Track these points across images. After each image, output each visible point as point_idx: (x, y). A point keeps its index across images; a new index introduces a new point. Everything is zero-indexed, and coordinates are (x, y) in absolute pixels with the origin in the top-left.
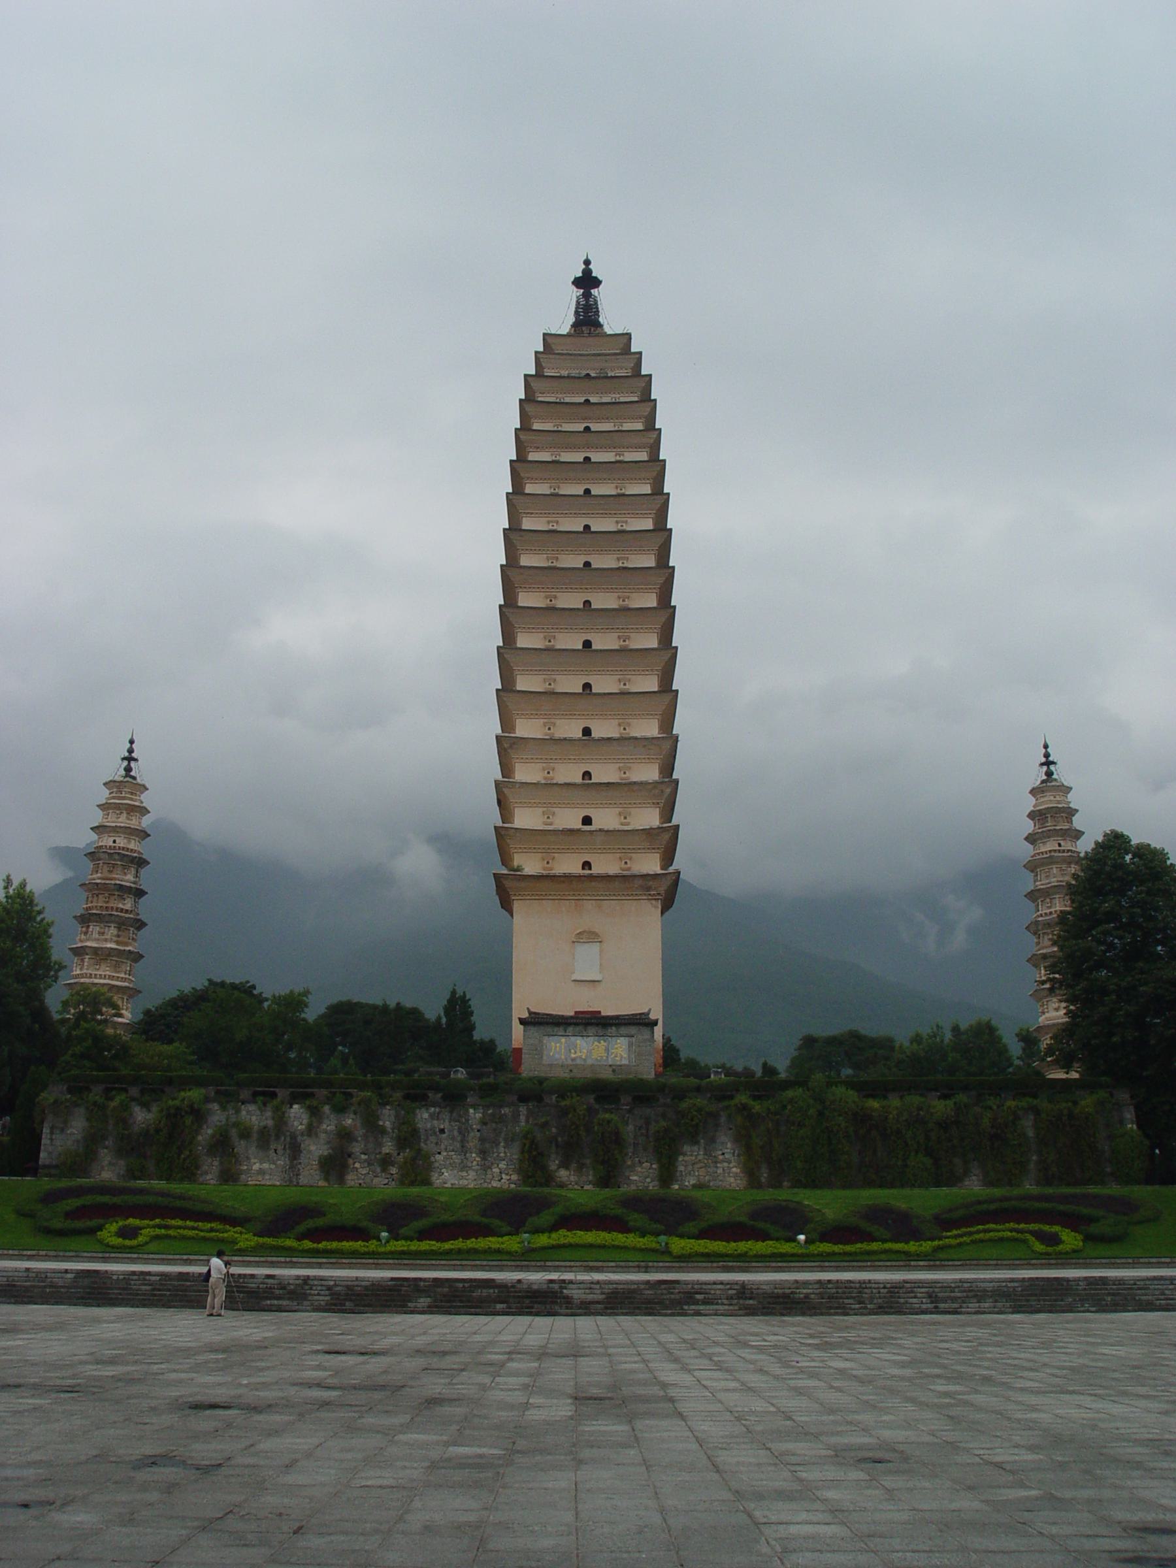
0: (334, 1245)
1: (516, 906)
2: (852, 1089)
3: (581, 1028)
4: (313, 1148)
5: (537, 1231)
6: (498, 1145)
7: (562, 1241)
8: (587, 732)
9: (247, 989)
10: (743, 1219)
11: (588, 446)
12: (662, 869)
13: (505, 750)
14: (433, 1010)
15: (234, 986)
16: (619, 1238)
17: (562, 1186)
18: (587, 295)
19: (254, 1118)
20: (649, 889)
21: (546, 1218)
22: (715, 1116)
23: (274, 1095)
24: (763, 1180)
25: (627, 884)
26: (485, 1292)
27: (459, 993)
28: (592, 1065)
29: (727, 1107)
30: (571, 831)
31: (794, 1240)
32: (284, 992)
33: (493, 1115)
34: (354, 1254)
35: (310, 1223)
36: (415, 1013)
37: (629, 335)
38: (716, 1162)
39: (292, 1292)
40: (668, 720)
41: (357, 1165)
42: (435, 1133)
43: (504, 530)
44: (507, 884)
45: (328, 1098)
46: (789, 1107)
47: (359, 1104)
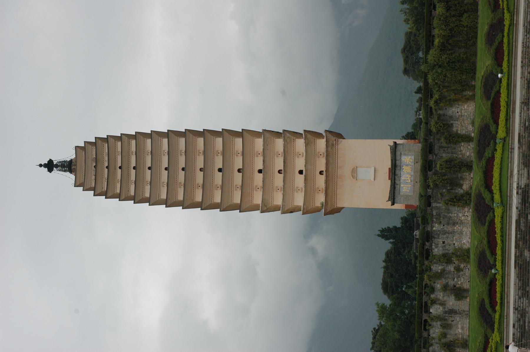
0: (498, 295)
1: (339, 205)
2: (429, 52)
3: (396, 177)
4: (451, 304)
5: (492, 199)
6: (451, 217)
7: (498, 188)
8: (260, 171)
9: (376, 331)
10: (489, 103)
11: (128, 167)
12: (323, 138)
13: (267, 209)
14: (387, 245)
15: (374, 338)
16: (497, 161)
17: (471, 188)
18: (57, 166)
19: (437, 331)
20: (333, 145)
21: (486, 195)
22: (439, 116)
23: (426, 321)
24: (471, 94)
25: (330, 155)
26: (522, 224)
27: (379, 233)
28: (414, 173)
29: (436, 110)
30: (306, 179)
31: (501, 79)
32: (377, 315)
33: (436, 218)
34: (503, 286)
35: (488, 306)
36: (387, 254)
37: (76, 147)
38: (462, 116)
39: (522, 317)
40: (256, 134)
41: (459, 283)
42: (445, 246)
43: (166, 207)
44: (329, 209)
45: (428, 295)
46: (436, 81)
47: (430, 281)
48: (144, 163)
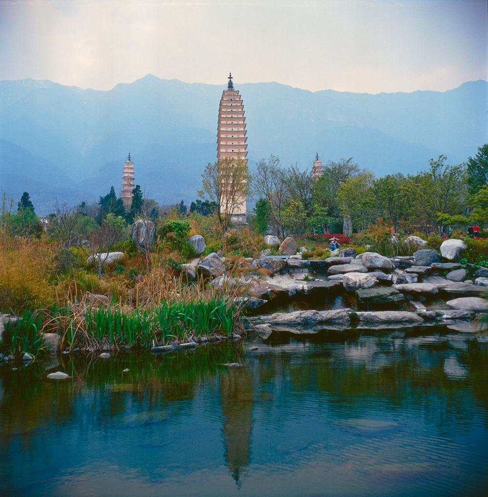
11: (233, 114)
18: (230, 80)
48: (234, 121)
